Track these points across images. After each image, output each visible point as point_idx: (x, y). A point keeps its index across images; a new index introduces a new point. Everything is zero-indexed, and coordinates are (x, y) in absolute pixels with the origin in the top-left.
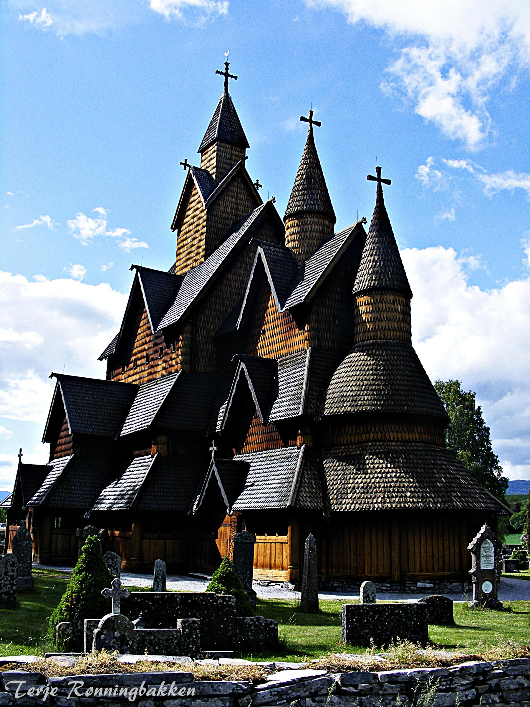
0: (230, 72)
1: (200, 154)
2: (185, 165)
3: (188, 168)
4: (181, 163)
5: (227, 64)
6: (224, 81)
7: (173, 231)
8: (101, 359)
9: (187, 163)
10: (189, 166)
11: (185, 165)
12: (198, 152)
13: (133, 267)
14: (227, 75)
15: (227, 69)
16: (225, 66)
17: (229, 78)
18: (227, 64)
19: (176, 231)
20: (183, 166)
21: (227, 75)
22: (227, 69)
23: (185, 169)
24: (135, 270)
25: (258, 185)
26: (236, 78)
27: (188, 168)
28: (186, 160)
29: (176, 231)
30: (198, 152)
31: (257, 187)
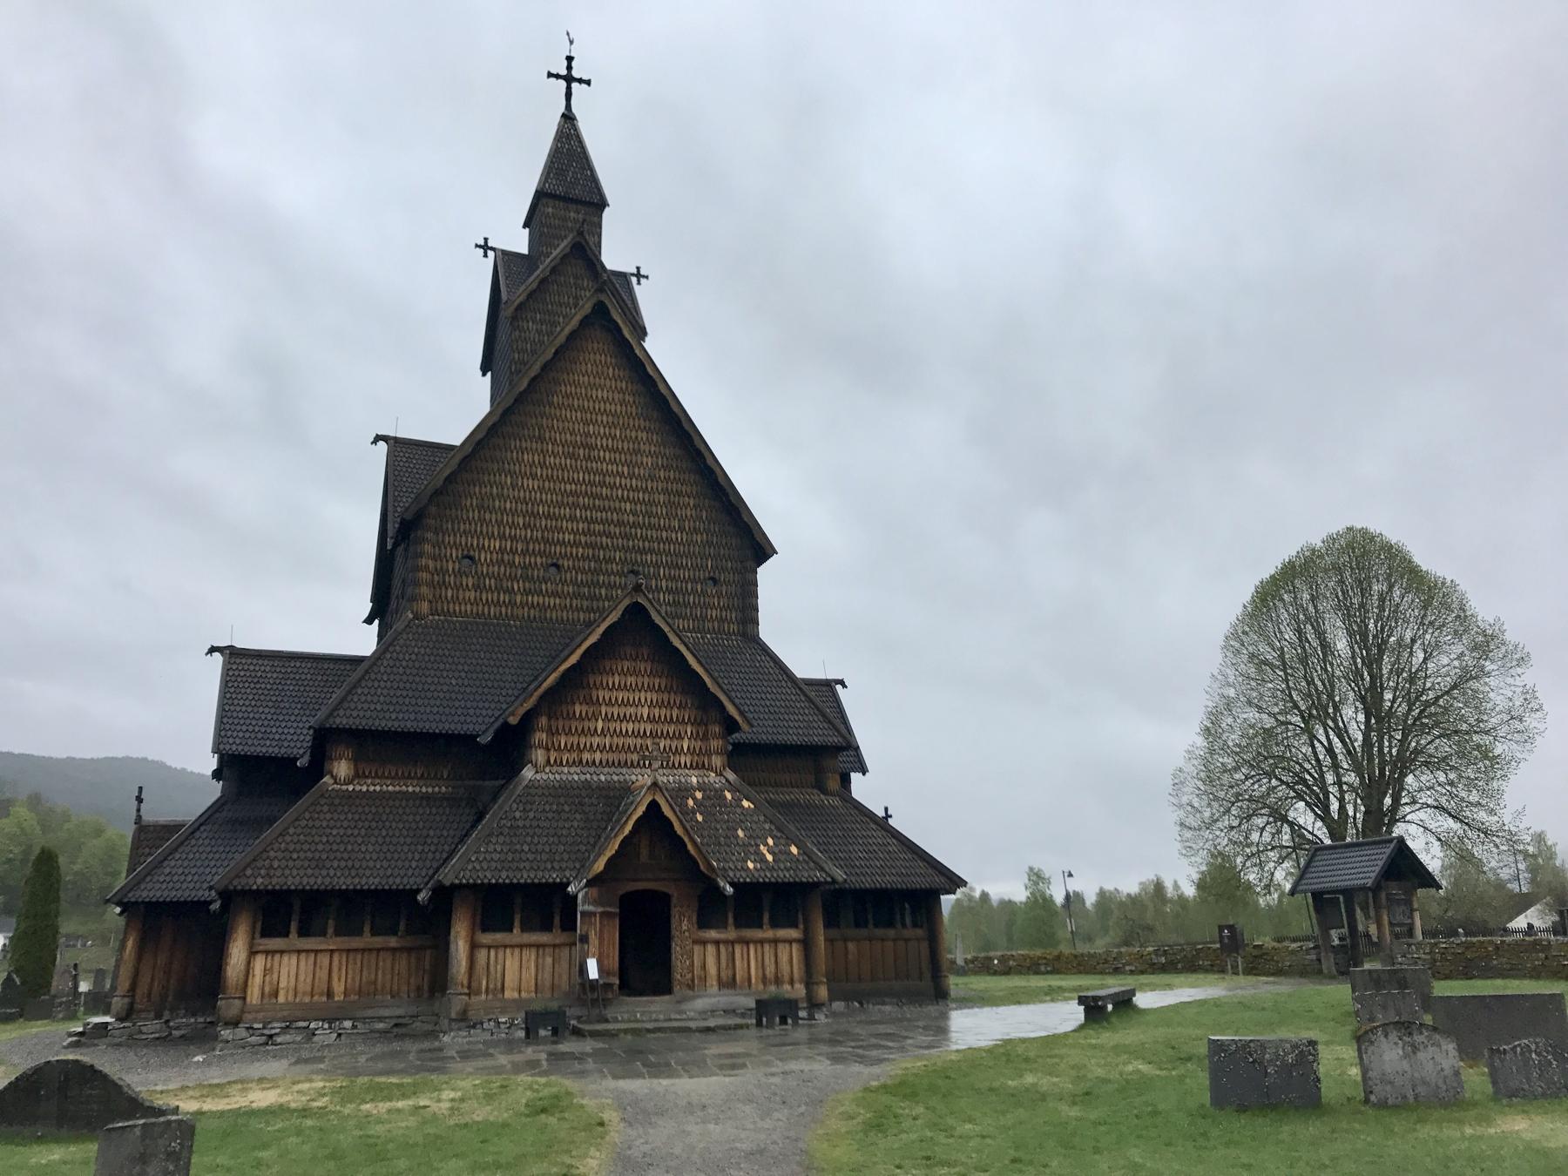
0: (576, 74)
1: (527, 230)
2: (485, 247)
3: (491, 254)
4: (477, 246)
5: (570, 59)
6: (564, 91)
7: (484, 375)
8: (369, 621)
9: (490, 245)
10: (492, 249)
11: (485, 247)
12: (524, 227)
13: (378, 438)
14: (569, 79)
15: (569, 68)
16: (565, 63)
17: (575, 85)
18: (570, 59)
19: (489, 374)
20: (482, 250)
21: (569, 79)
22: (569, 68)
23: (486, 255)
25: (638, 275)
26: (588, 83)
27: (491, 254)
28: (486, 239)
29: (489, 374)
30: (524, 227)
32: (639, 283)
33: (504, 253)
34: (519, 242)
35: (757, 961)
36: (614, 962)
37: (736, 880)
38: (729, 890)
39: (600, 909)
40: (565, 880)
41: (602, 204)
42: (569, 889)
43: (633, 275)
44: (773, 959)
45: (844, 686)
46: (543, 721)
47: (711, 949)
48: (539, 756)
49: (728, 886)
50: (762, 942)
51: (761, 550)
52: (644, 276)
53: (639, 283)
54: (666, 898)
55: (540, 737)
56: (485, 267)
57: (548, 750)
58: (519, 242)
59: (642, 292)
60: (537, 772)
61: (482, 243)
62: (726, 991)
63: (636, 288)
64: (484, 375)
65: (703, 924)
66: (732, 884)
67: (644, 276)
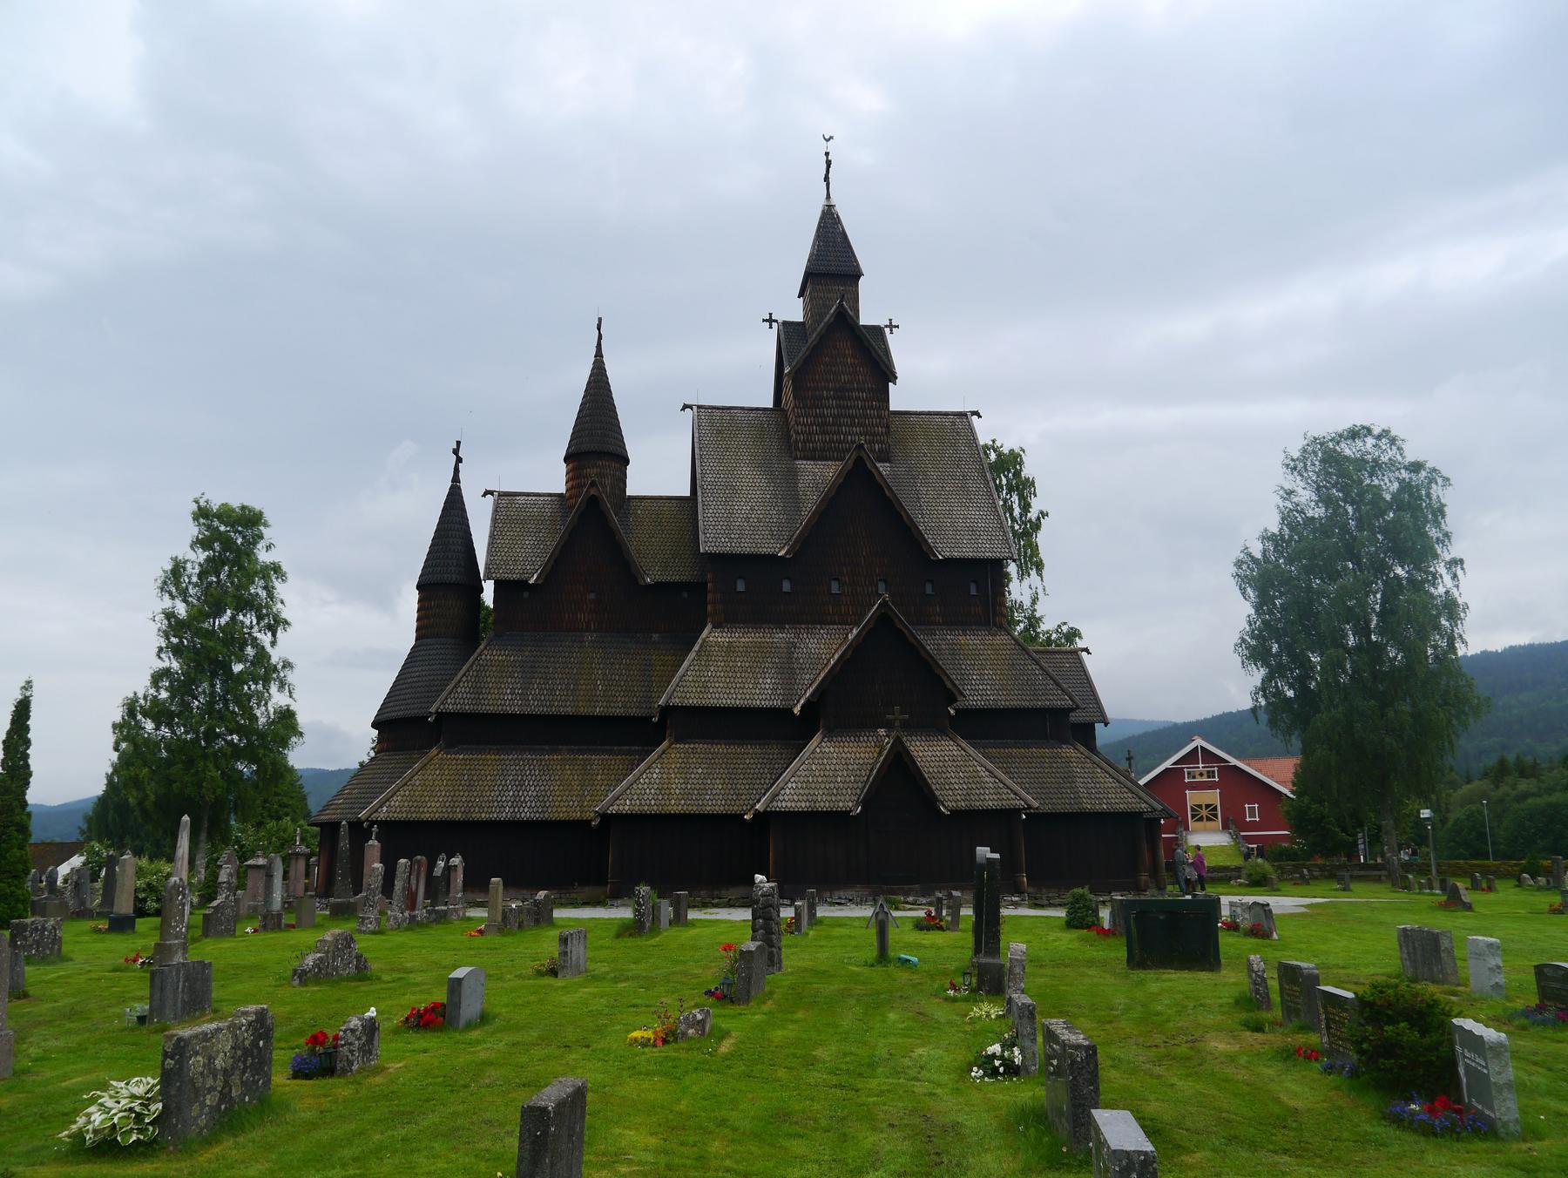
3: (775, 325)
4: (764, 320)
5: (827, 154)
9: (773, 318)
10: (776, 321)
11: (770, 321)
12: (799, 297)
23: (771, 327)
25: (891, 326)
28: (771, 314)
30: (799, 297)
31: (891, 330)
33: (785, 323)
34: (794, 311)
41: (856, 275)
43: (886, 326)
58: (794, 311)
59: (893, 340)
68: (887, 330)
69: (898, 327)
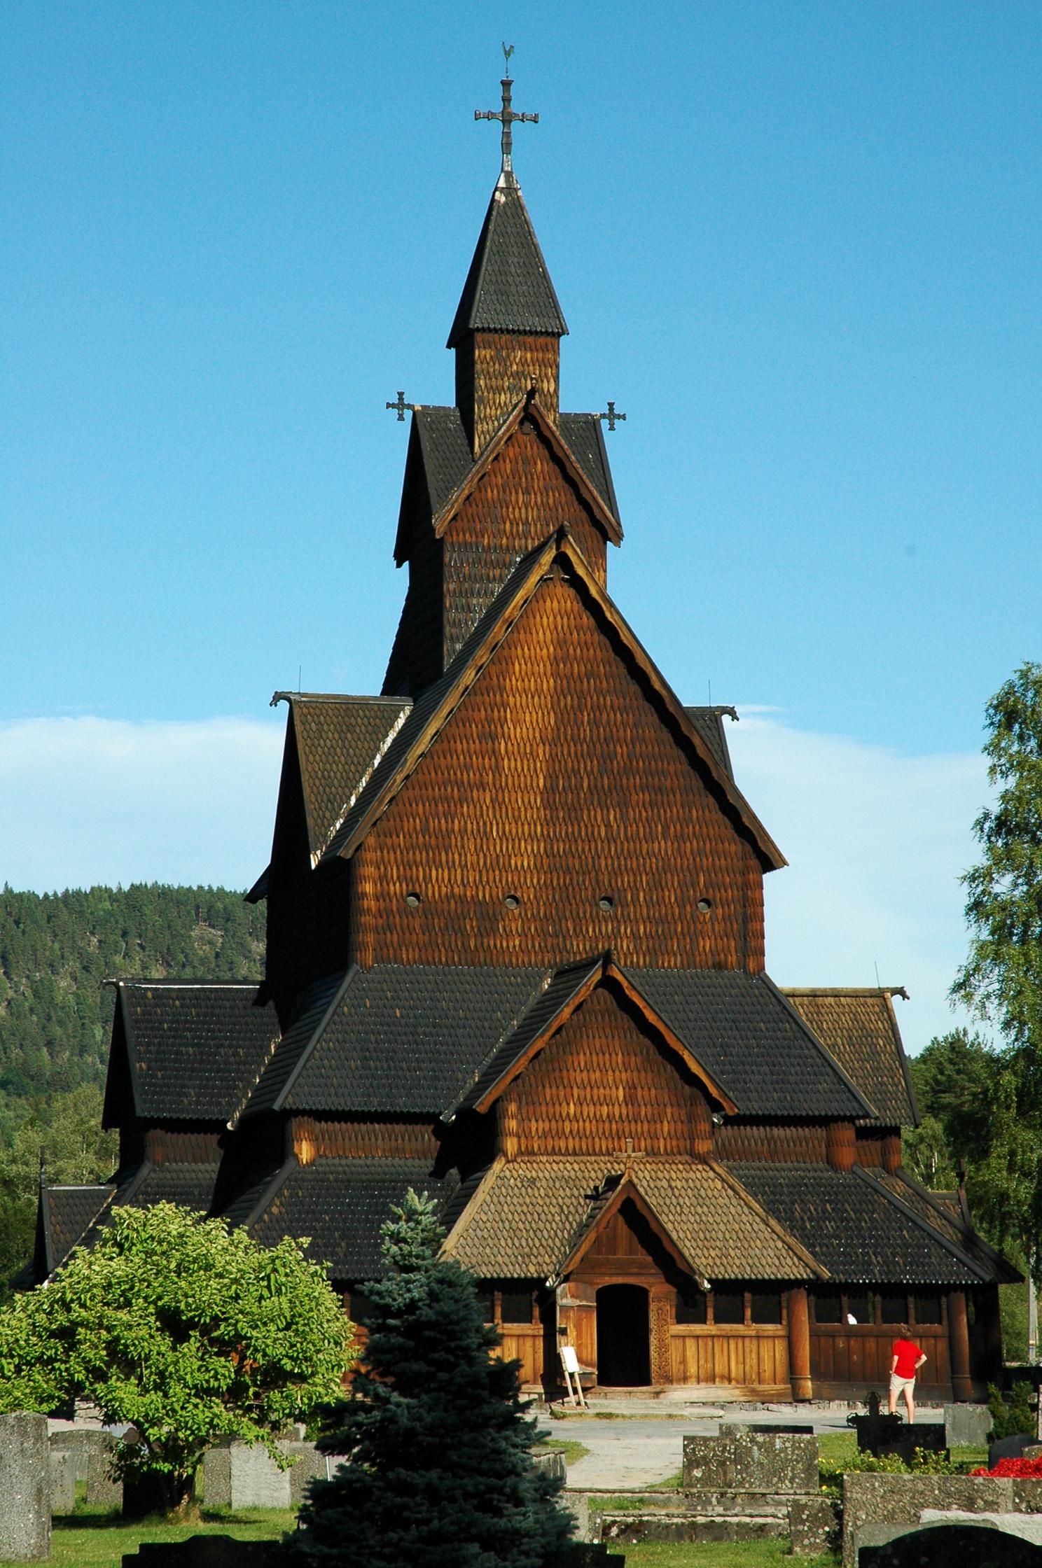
1: (453, 350)
4: (389, 405)
5: (506, 84)
10: (410, 407)
11: (400, 405)
12: (449, 346)
13: (278, 697)
15: (506, 100)
18: (506, 84)
21: (507, 119)
22: (506, 100)
23: (401, 418)
24: (284, 706)
25: (612, 415)
27: (408, 414)
28: (401, 394)
30: (449, 346)
32: (612, 428)
35: (737, 1355)
36: (593, 1353)
37: (714, 1276)
38: (707, 1285)
39: (578, 1302)
40: (543, 1275)
42: (548, 1284)
43: (603, 416)
44: (754, 1355)
45: (905, 996)
46: (513, 1108)
47: (691, 1345)
48: (511, 1145)
49: (706, 1282)
50: (743, 1337)
51: (768, 860)
52: (619, 417)
53: (612, 428)
54: (644, 1293)
55: (512, 1124)
56: (404, 431)
57: (519, 1138)
59: (612, 441)
60: (508, 1162)
61: (396, 402)
62: (703, 1385)
63: (607, 436)
64: (399, 565)
65: (680, 1320)
66: (710, 1281)
67: (619, 417)
68: (605, 424)
69: (624, 417)
